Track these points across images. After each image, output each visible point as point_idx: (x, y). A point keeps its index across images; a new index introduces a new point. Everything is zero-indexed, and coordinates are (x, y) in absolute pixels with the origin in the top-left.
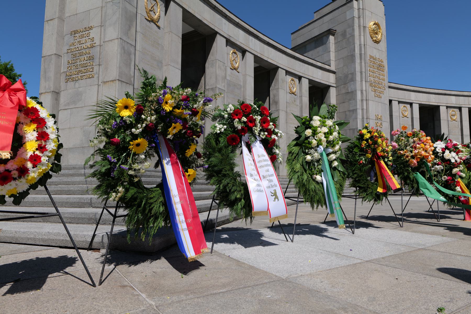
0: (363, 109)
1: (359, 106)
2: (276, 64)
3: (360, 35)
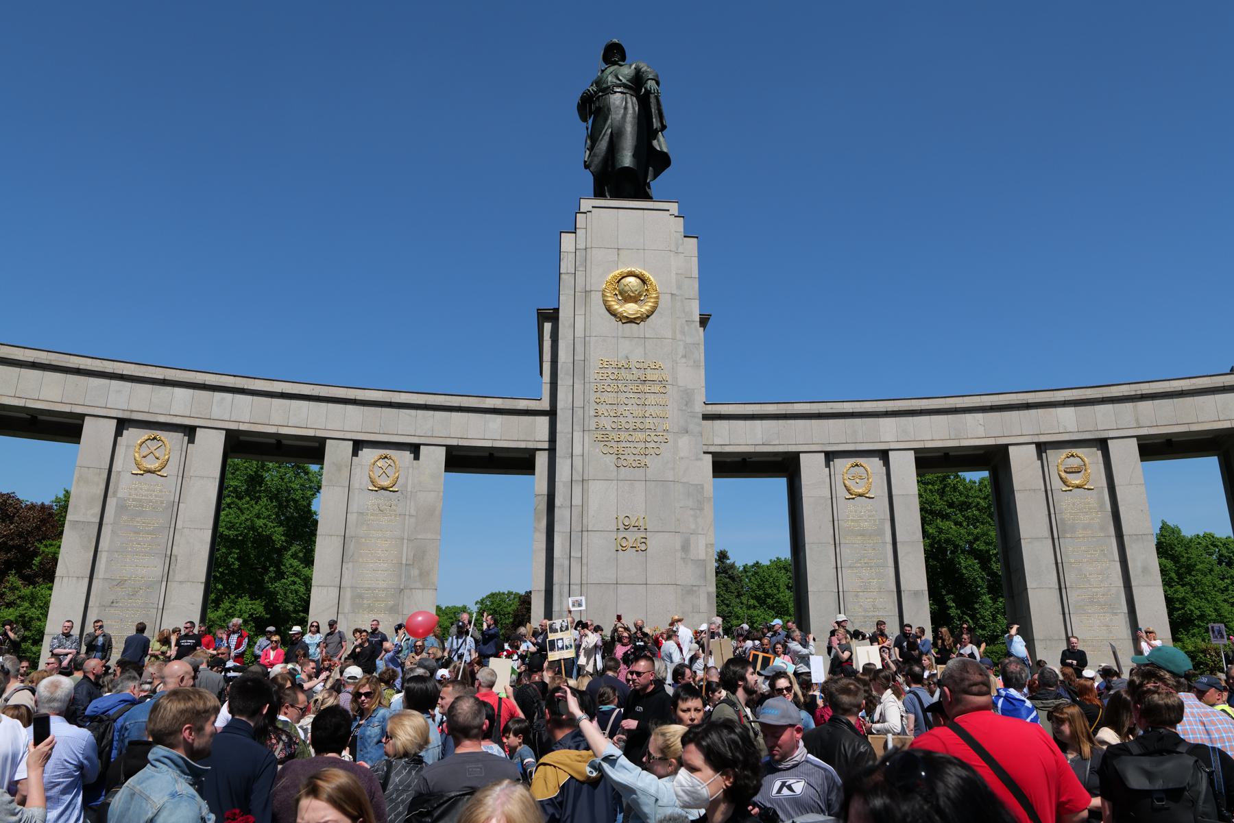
2: (311, 433)
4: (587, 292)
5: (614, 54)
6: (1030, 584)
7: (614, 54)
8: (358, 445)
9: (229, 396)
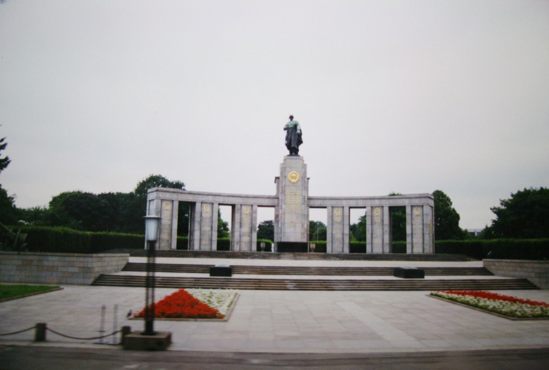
4: (285, 177)
5: (291, 118)
7: (291, 118)
8: (241, 205)
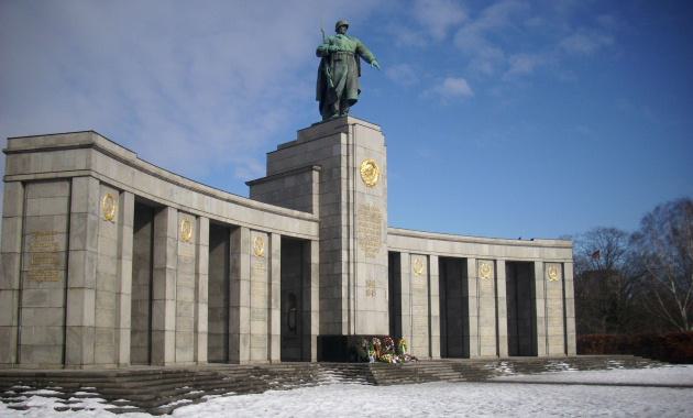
0: (349, 274)
1: (344, 270)
2: (236, 223)
3: (348, 179)
6: (471, 314)
7: (340, 28)
9: (209, 198)
